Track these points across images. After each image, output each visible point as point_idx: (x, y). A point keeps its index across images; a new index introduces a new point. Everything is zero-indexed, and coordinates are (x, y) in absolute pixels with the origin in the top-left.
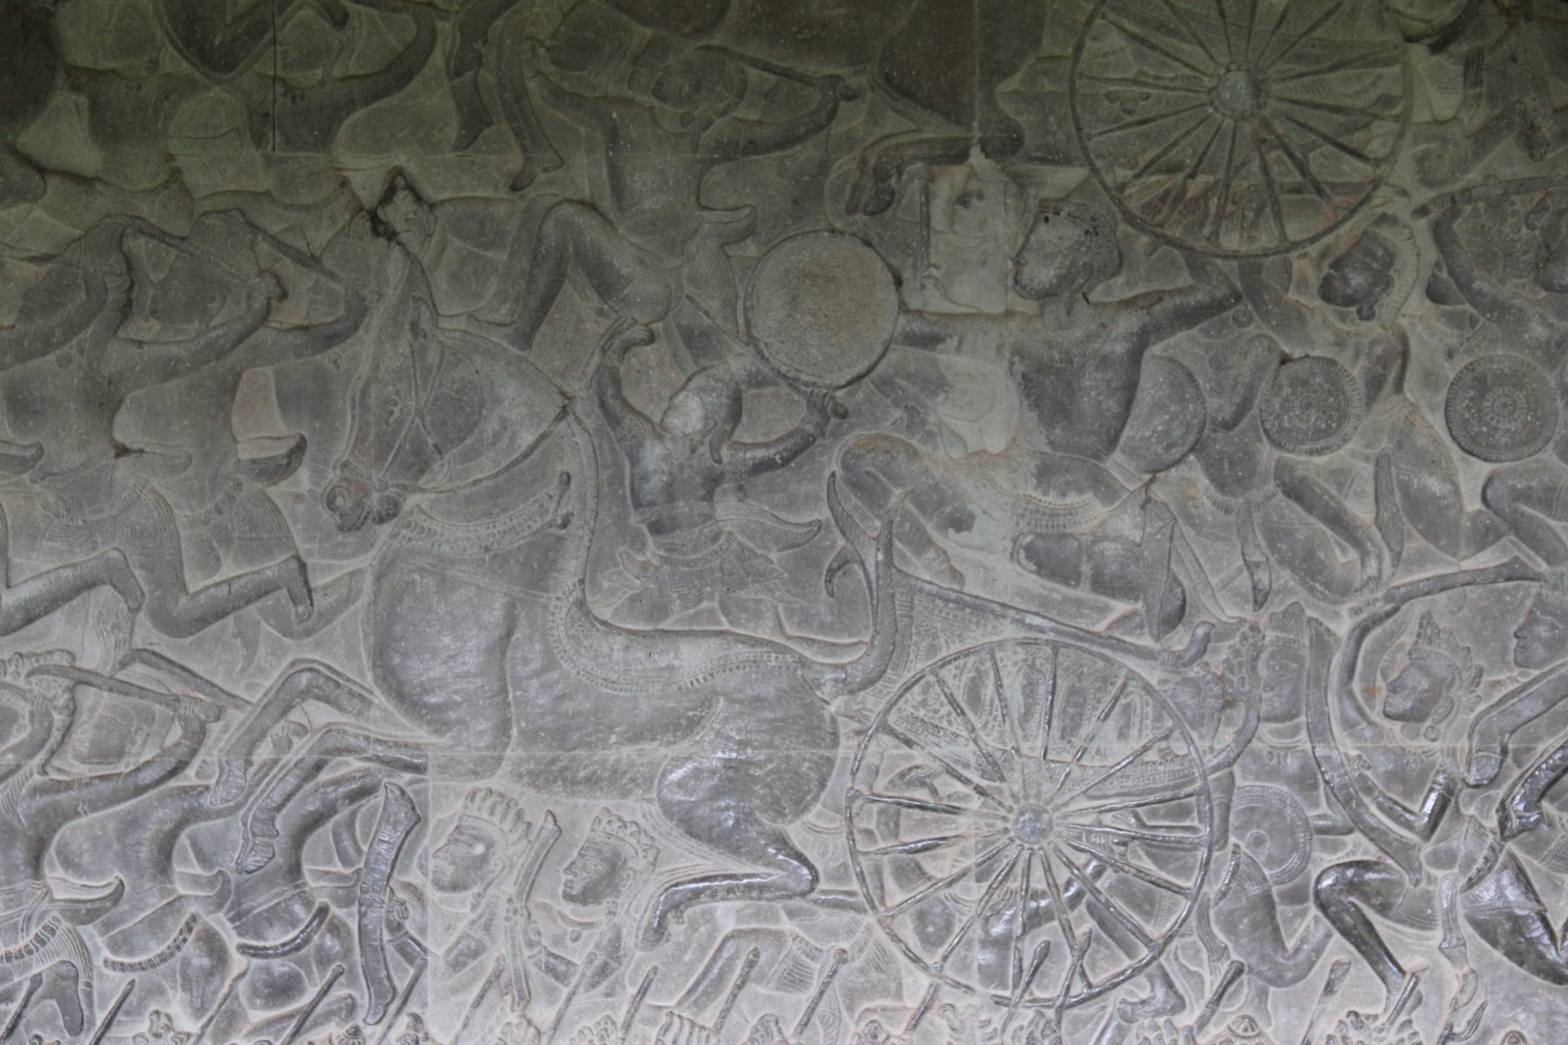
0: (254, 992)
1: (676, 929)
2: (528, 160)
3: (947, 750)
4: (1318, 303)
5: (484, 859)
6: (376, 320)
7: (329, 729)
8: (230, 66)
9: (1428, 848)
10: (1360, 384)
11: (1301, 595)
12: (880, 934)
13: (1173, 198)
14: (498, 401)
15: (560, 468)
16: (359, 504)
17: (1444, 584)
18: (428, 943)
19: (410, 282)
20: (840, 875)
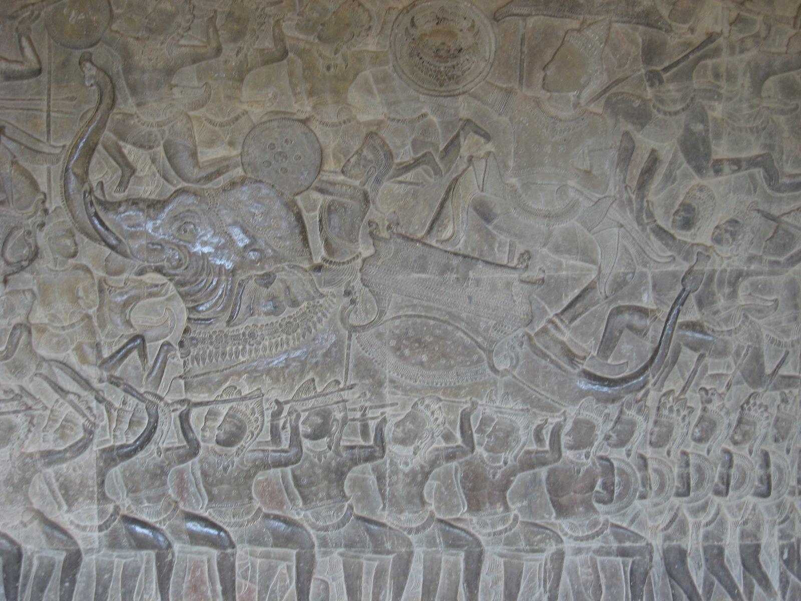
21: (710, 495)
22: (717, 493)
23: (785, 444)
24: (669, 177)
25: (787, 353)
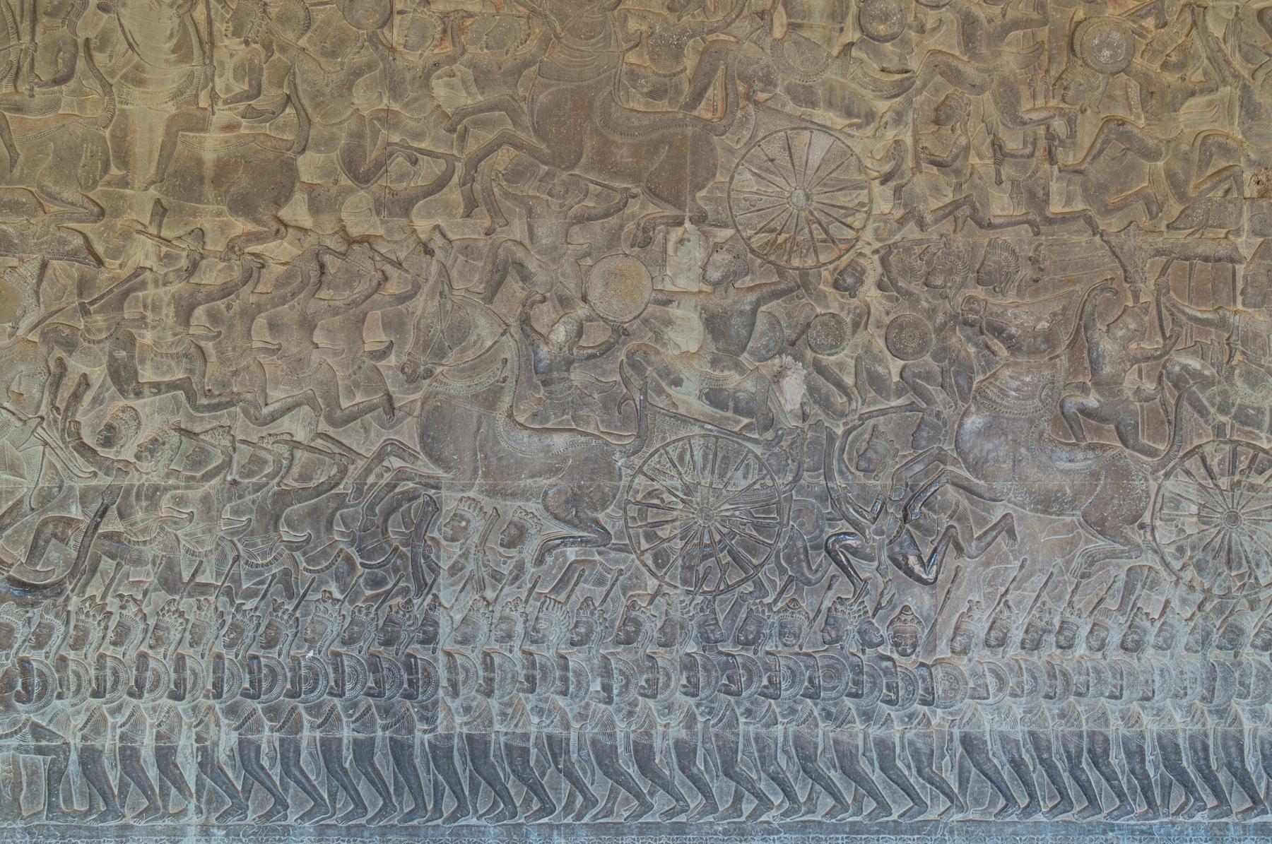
0: (366, 584)
1: (549, 559)
2: (493, 222)
3: (669, 483)
4: (832, 290)
5: (465, 528)
6: (426, 289)
7: (400, 470)
8: (367, 181)
9: (874, 527)
10: (850, 325)
11: (823, 417)
12: (637, 562)
13: (771, 244)
14: (476, 327)
15: (503, 356)
16: (414, 371)
17: (883, 412)
18: (441, 564)
19: (440, 274)
20: (620, 535)
21: (125, 696)
22: (131, 694)
23: (200, 649)
24: (97, 400)
25: (201, 562)
